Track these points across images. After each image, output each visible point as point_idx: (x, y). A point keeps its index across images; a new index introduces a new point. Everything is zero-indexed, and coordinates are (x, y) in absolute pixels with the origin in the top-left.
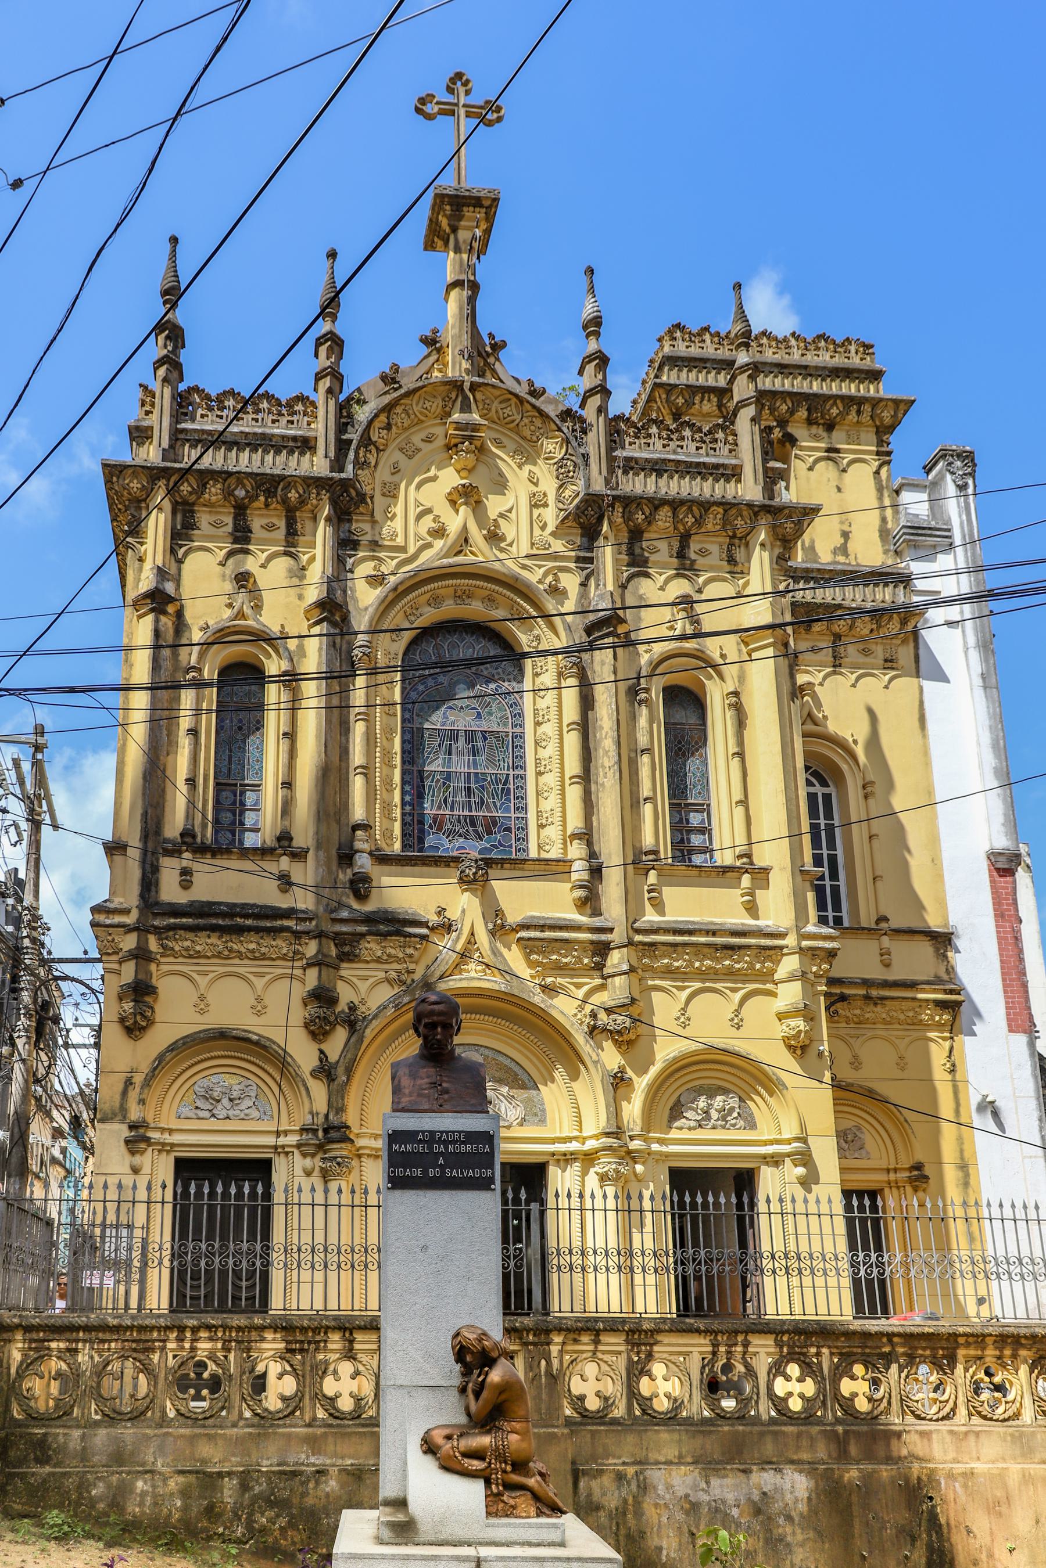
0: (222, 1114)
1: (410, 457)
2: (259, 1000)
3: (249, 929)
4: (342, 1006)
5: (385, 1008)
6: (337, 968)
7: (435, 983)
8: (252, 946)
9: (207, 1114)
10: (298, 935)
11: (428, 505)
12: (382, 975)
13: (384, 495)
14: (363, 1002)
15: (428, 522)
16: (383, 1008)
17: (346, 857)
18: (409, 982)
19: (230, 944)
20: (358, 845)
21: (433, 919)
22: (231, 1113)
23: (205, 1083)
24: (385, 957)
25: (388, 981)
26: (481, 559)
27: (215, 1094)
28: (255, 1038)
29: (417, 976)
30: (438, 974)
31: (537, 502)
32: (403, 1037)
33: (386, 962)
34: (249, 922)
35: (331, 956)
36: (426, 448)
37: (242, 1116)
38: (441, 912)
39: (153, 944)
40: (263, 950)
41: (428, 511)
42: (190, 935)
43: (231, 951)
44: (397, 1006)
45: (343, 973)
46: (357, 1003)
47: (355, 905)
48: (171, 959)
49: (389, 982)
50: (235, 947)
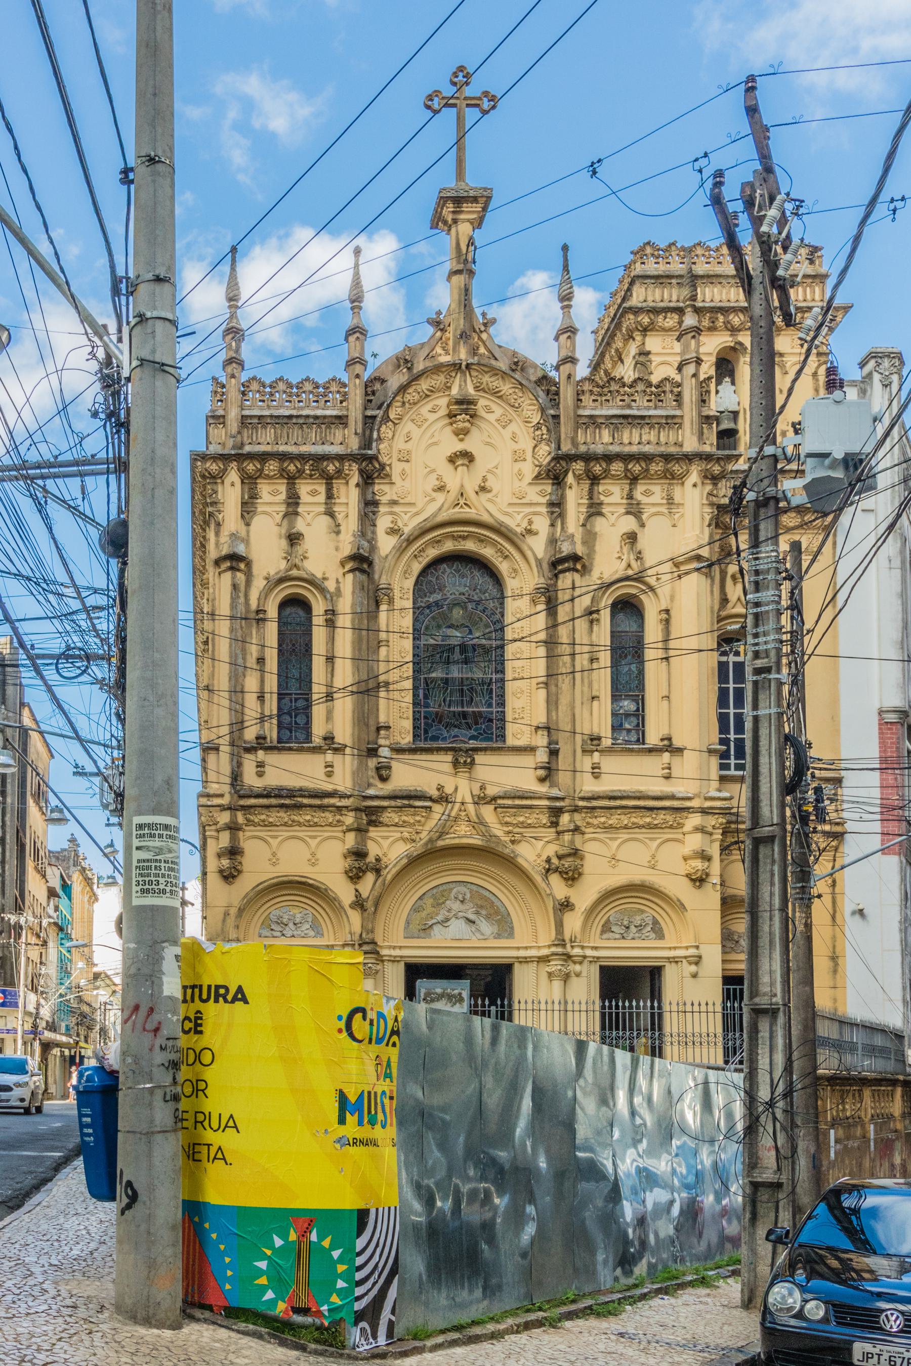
0: (289, 933)
1: (419, 426)
2: (313, 854)
3: (306, 806)
4: (371, 858)
6: (367, 831)
8: (308, 818)
9: (279, 934)
10: (339, 809)
11: (433, 467)
13: (399, 460)
15: (433, 482)
17: (372, 752)
19: (293, 817)
20: (381, 742)
21: (435, 793)
22: (295, 933)
23: (277, 912)
25: (402, 839)
26: (473, 511)
27: (285, 921)
31: (518, 457)
34: (305, 801)
36: (432, 417)
38: (440, 788)
39: (240, 818)
40: (316, 820)
41: (433, 471)
42: (265, 811)
43: (293, 821)
45: (371, 834)
47: (380, 785)
48: (252, 828)
50: (296, 818)
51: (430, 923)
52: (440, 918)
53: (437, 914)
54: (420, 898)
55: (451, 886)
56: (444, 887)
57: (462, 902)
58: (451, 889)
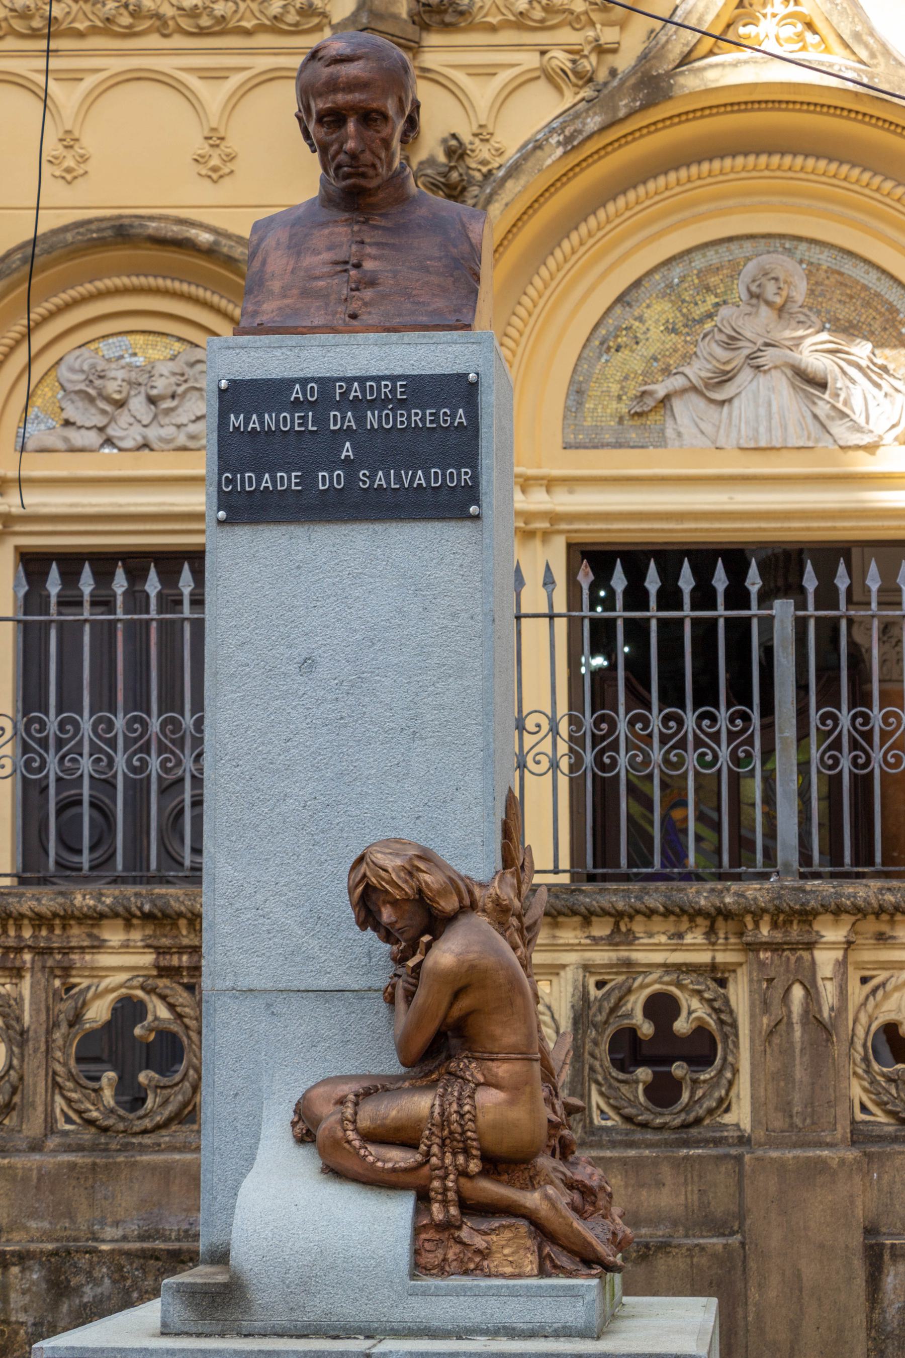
5: (538, 147)
7: (670, 74)
12: (531, 60)
14: (483, 135)
16: (535, 146)
18: (602, 75)
24: (538, 14)
28: (205, 238)
29: (624, 62)
30: (676, 51)
32: (592, 222)
33: (542, 27)
35: (395, 17)
37: (182, 440)
44: (568, 140)
46: (466, 137)
49: (550, 79)
51: (661, 390)
52: (697, 371)
53: (687, 358)
54: (620, 299)
55: (738, 251)
56: (711, 255)
57: (781, 310)
58: (735, 270)
